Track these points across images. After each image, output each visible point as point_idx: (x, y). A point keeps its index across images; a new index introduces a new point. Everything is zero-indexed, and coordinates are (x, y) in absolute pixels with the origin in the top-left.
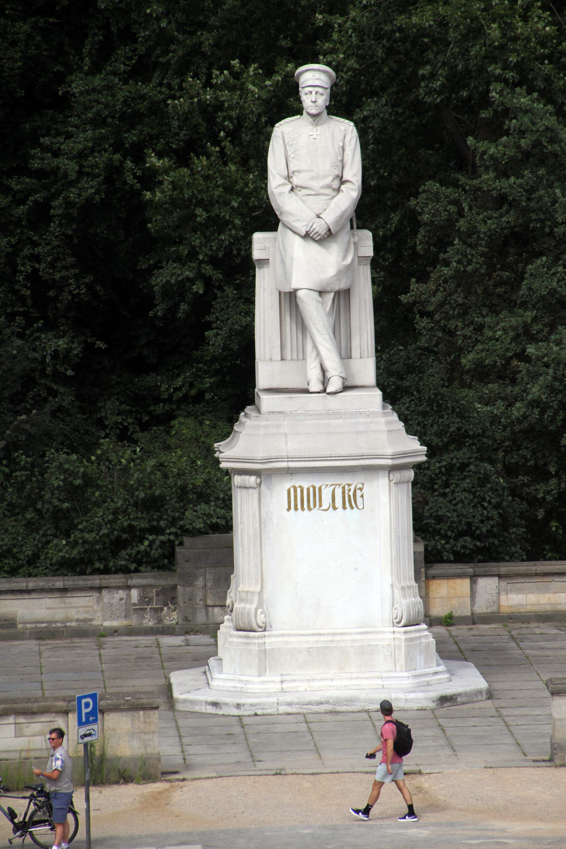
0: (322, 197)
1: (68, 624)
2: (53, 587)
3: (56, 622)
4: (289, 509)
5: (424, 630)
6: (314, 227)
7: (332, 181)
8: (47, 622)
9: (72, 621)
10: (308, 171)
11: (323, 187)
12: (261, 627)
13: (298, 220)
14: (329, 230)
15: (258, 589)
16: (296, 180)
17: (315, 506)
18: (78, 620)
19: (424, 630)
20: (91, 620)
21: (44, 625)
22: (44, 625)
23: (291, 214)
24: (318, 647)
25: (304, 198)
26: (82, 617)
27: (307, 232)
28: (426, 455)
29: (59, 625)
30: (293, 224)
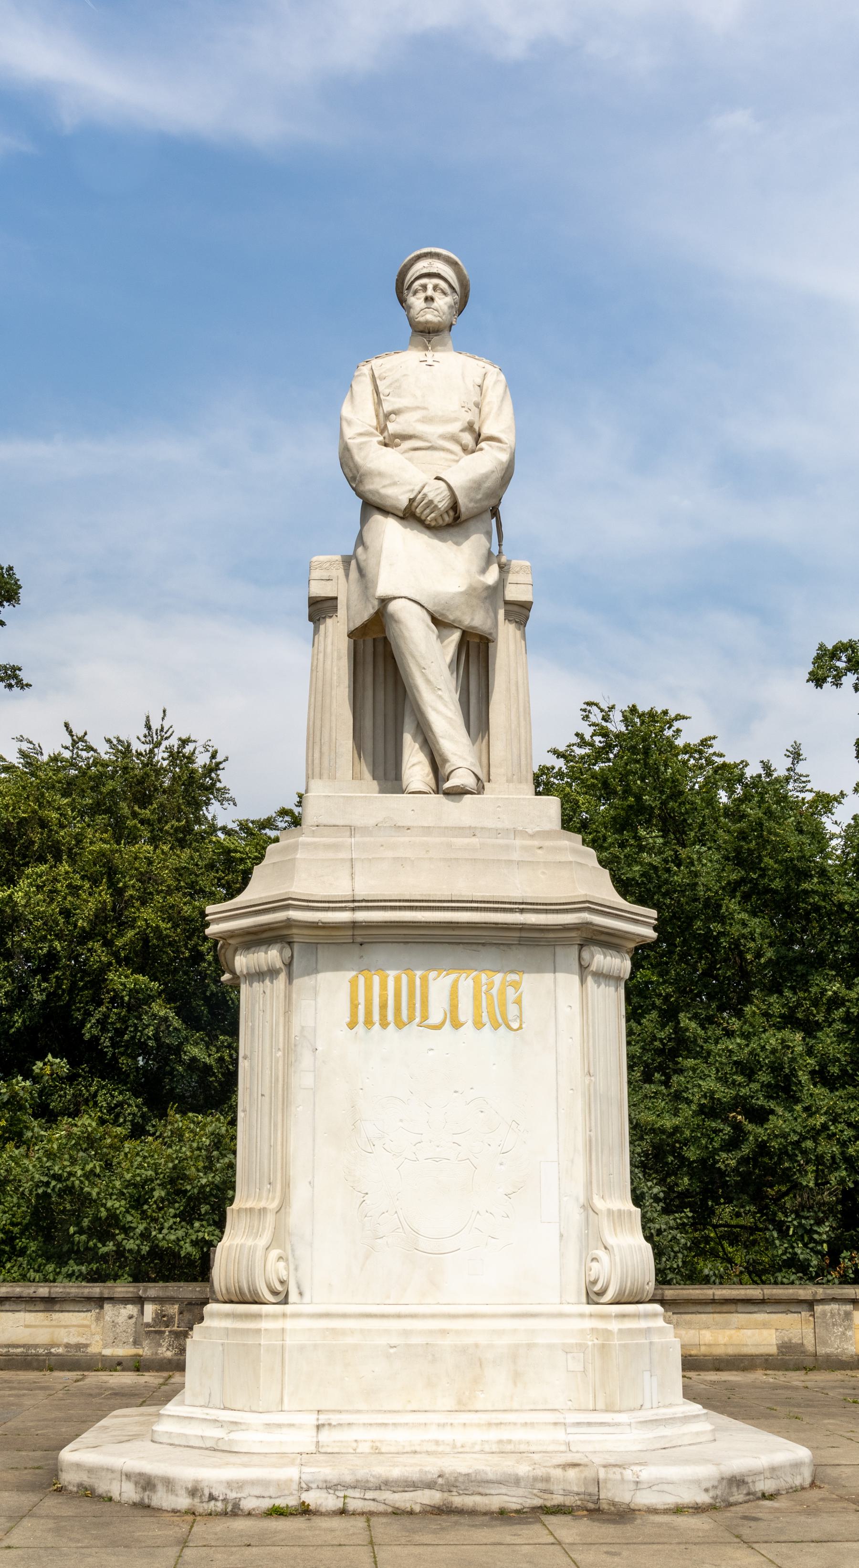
0: (442, 454)
1: (53, 1350)
2: (34, 1295)
3: (36, 1346)
4: (352, 1025)
5: (655, 1315)
6: (425, 491)
7: (462, 431)
8: (24, 1346)
9: (58, 1346)
10: (417, 408)
11: (443, 437)
12: (275, 1293)
13: (394, 484)
14: (454, 506)
15: (274, 1205)
16: (392, 427)
17: (411, 1019)
18: (67, 1346)
19: (655, 1315)
20: (86, 1346)
21: (19, 1350)
22: (19, 1350)
23: (380, 474)
24: (408, 1346)
25: (407, 455)
26: (73, 1340)
27: (411, 501)
28: (655, 929)
29: (41, 1351)
30: (383, 491)
